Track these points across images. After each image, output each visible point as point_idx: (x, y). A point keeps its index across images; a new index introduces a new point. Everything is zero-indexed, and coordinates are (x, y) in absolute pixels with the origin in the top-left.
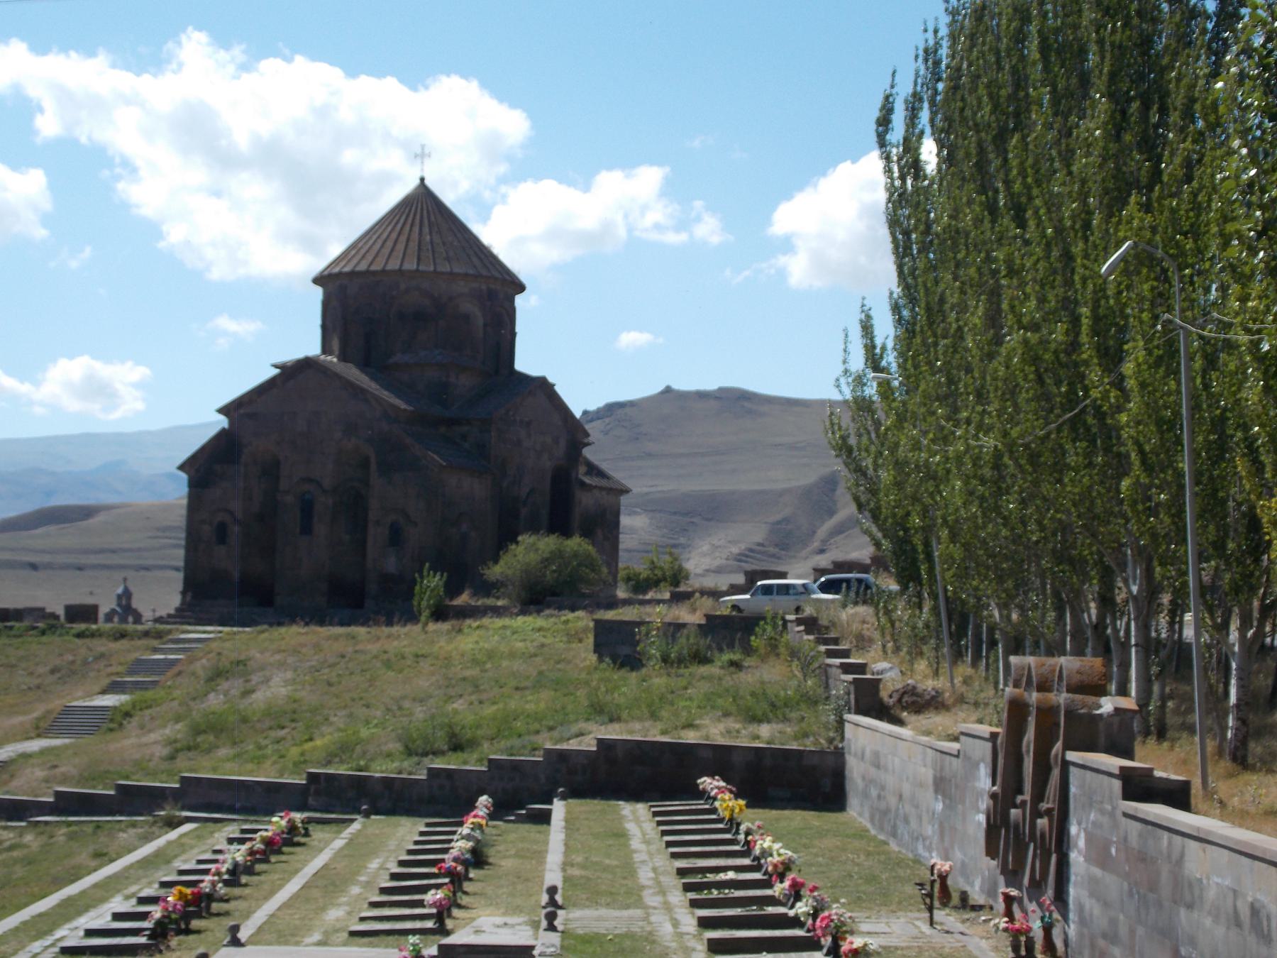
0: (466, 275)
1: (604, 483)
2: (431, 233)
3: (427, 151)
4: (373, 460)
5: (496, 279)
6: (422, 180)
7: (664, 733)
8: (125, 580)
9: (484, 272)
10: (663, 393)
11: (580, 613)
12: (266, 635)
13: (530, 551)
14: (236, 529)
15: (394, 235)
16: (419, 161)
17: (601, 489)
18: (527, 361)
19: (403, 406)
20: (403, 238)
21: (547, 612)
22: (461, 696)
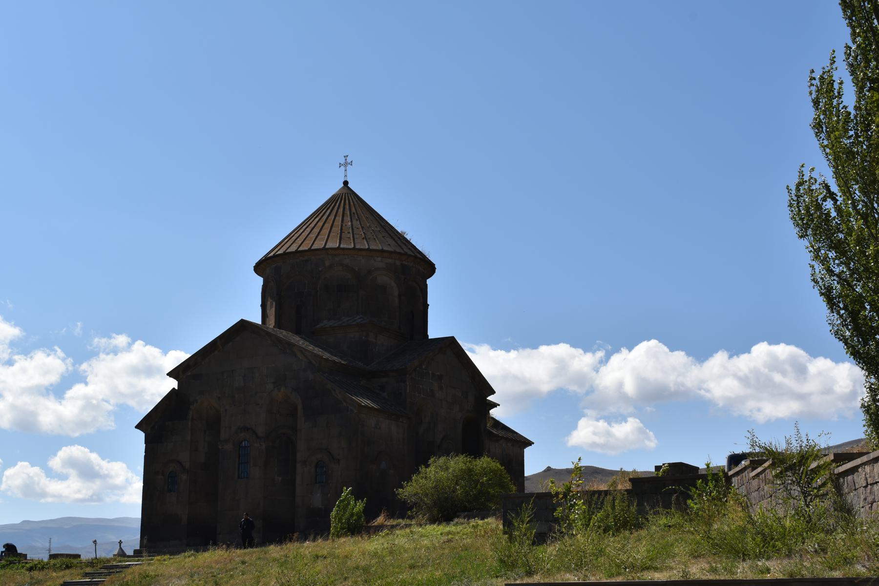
0: (382, 251)
1: (510, 435)
2: (351, 221)
3: (349, 160)
4: (300, 407)
5: (410, 256)
6: (346, 183)
7: (611, 576)
8: (120, 542)
9: (398, 250)
10: (545, 471)
11: (490, 520)
12: (193, 558)
13: (441, 471)
14: (184, 477)
15: (321, 224)
16: (343, 168)
17: (507, 440)
18: (437, 328)
19: (326, 355)
20: (328, 225)
21: (456, 520)
22: (346, 579)
